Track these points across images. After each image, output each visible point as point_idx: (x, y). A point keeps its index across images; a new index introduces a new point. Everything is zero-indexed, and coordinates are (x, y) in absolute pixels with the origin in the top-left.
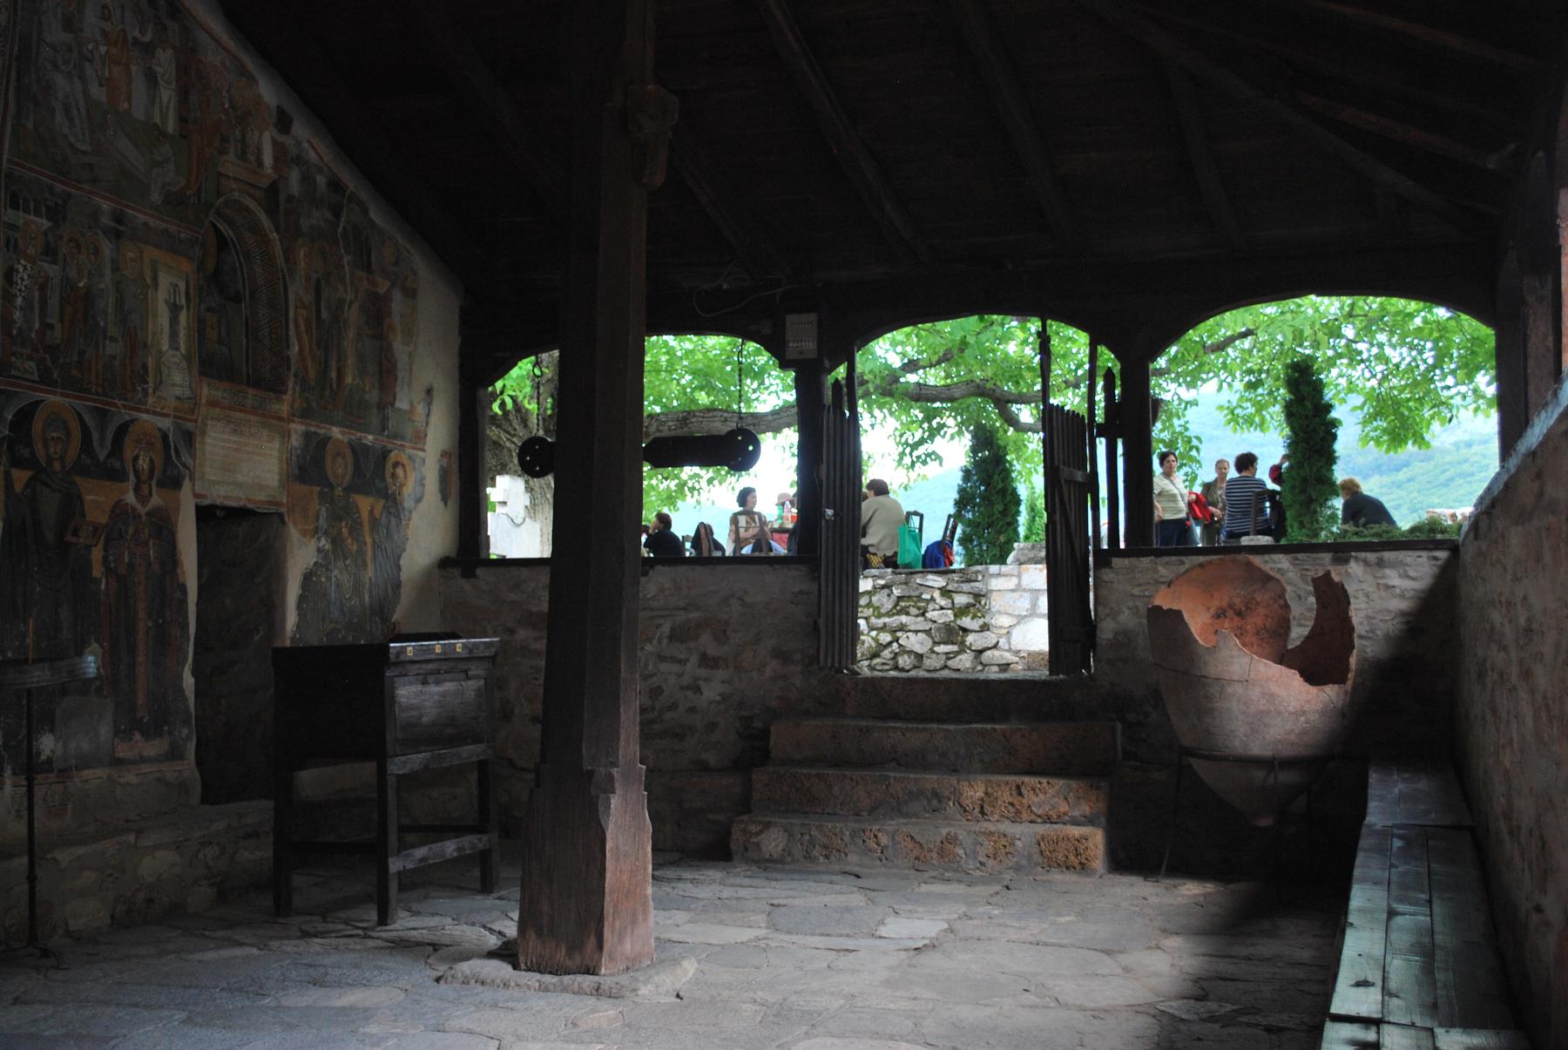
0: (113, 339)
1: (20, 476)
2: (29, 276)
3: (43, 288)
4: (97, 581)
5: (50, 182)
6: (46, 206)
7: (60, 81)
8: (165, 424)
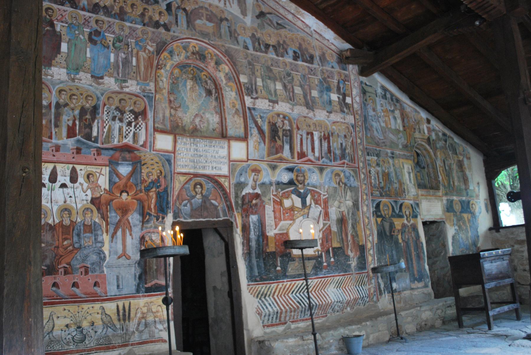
0: (396, 183)
1: (379, 220)
3: (378, 174)
4: (401, 244)
7: (374, 124)
8: (411, 202)
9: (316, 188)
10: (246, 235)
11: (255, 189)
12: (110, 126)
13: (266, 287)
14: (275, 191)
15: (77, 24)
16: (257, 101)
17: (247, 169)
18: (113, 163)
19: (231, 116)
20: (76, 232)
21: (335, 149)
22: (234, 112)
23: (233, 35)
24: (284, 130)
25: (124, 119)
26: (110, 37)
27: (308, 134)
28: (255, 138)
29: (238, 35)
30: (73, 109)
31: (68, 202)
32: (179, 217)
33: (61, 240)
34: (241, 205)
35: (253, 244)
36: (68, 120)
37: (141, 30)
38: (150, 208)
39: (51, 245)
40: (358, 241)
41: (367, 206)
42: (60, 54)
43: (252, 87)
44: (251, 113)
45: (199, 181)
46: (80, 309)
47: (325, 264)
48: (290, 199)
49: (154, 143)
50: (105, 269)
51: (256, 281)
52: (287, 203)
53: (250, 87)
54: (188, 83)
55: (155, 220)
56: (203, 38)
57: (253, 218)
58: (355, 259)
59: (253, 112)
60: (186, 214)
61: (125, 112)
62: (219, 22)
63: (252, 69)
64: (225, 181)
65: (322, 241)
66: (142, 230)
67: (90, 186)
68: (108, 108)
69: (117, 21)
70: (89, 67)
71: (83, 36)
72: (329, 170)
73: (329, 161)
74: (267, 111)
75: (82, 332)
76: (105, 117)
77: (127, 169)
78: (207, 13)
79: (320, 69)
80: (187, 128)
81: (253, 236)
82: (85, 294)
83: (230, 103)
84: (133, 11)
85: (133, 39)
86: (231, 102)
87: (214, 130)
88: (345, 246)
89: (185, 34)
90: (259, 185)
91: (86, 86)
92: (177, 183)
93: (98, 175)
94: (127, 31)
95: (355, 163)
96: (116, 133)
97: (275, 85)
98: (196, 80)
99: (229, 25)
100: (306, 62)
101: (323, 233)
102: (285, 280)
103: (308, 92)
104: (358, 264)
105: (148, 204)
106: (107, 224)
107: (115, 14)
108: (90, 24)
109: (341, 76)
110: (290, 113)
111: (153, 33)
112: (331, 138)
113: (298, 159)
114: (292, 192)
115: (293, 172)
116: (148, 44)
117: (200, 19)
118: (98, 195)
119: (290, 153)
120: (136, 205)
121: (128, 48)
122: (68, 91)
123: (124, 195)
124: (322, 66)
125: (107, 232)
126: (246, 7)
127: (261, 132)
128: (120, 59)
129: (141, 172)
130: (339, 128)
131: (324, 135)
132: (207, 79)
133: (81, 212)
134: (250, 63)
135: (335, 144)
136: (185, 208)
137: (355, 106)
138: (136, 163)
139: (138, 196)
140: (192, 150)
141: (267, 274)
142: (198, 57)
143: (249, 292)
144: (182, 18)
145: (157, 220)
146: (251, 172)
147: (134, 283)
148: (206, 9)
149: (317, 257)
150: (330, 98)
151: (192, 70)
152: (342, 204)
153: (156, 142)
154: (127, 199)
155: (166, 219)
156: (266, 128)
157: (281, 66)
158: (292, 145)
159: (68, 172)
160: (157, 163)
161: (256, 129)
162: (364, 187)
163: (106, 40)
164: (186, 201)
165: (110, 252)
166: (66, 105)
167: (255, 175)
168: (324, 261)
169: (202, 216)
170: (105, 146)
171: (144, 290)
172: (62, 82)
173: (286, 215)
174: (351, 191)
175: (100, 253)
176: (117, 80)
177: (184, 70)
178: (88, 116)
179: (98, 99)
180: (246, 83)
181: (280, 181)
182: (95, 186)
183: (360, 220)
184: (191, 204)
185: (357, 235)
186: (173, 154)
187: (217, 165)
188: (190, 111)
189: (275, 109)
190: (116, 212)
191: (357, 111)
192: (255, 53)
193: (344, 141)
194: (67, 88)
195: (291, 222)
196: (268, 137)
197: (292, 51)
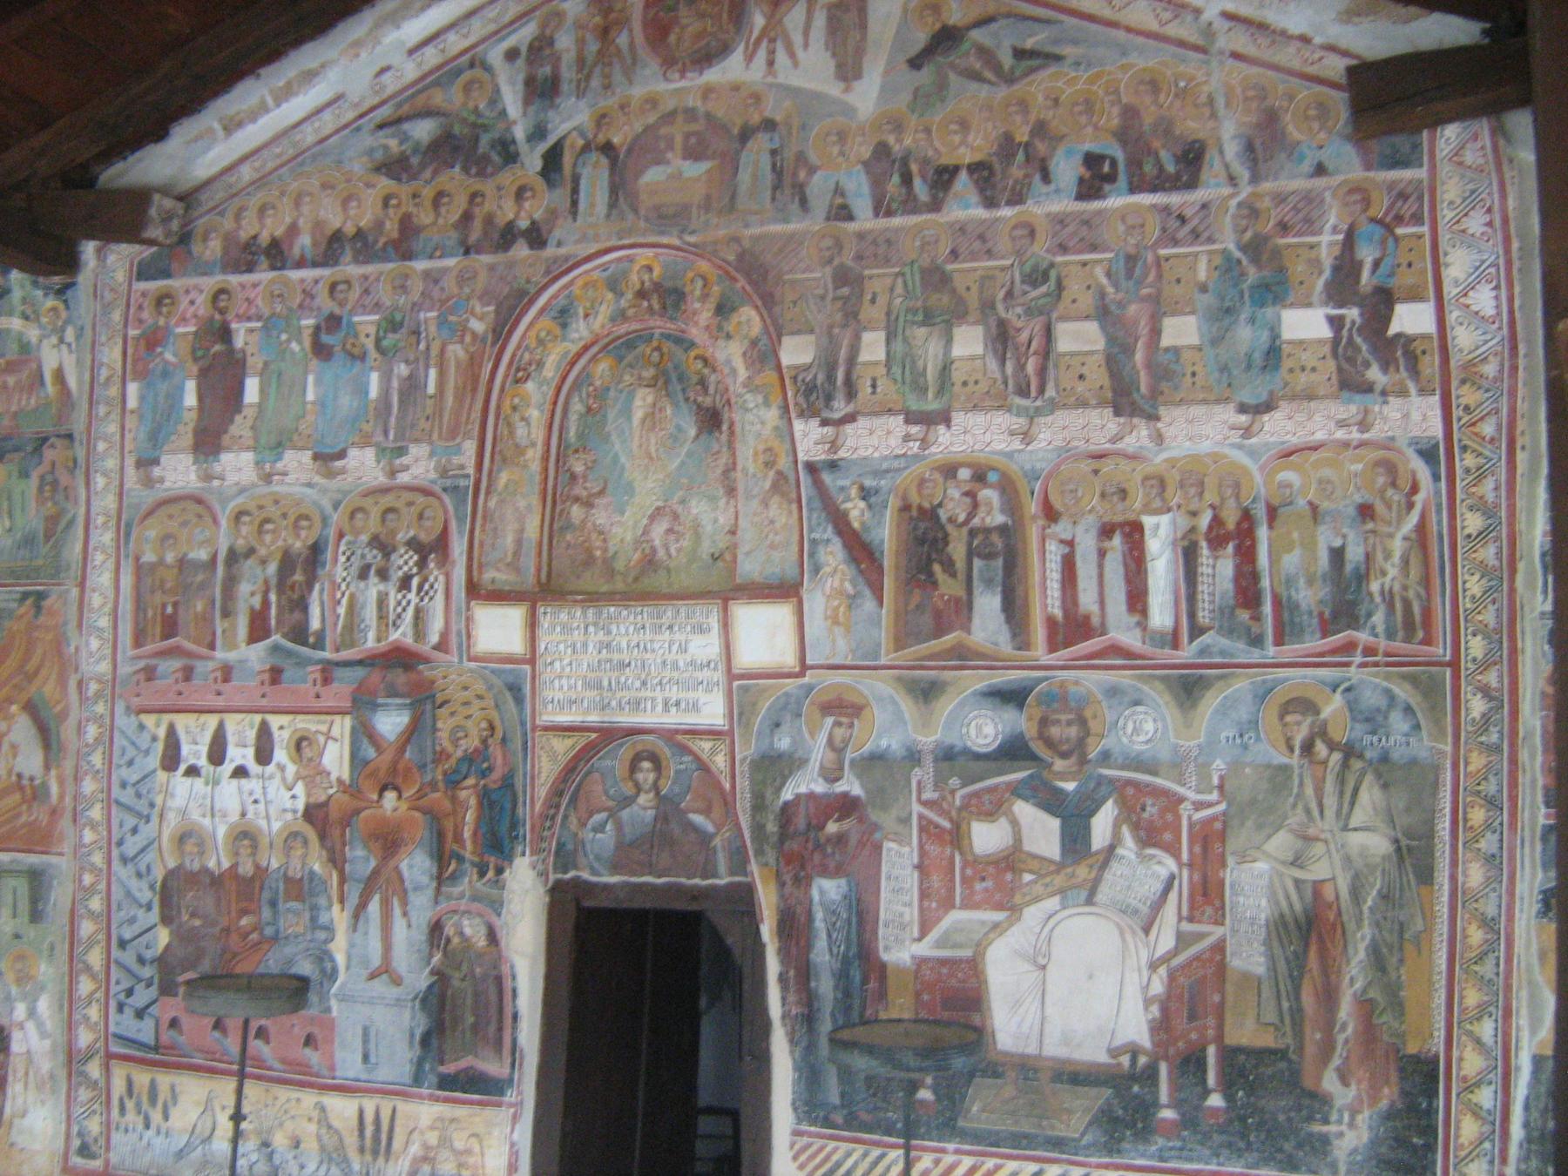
9: (1155, 773)
10: (794, 950)
11: (837, 779)
12: (352, 597)
13: (865, 1155)
14: (930, 786)
15: (285, 312)
16: (849, 429)
17: (799, 704)
18: (362, 704)
19: (755, 503)
20: (266, 895)
21: (1290, 582)
22: (768, 484)
23: (787, 179)
24: (973, 533)
25: (391, 572)
26: (367, 322)
27: (1107, 531)
28: (830, 584)
29: (812, 170)
30: (264, 562)
31: (250, 815)
32: (576, 867)
33: (234, 914)
34: (775, 839)
35: (825, 986)
36: (253, 594)
37: (454, 273)
38: (458, 838)
39: (214, 924)
40: (1402, 1036)
41: (1491, 860)
42: (240, 412)
43: (831, 378)
44: (818, 484)
45: (649, 747)
46: (270, 1102)
47: (1168, 1114)
49: (469, 636)
50: (334, 1003)
51: (827, 1122)
52: (987, 837)
53: (821, 378)
54: (638, 402)
55: (475, 877)
56: (662, 233)
57: (828, 890)
58: (1363, 1118)
59: (827, 477)
60: (598, 858)
61: (394, 549)
62: (737, 145)
63: (846, 299)
64: (713, 752)
65: (1165, 1010)
66: (436, 902)
67: (304, 773)
68: (349, 543)
69: (391, 266)
70: (309, 431)
71: (300, 342)
72: (1241, 685)
73: (1241, 645)
74: (896, 464)
75: (270, 1156)
76: (340, 573)
77: (398, 720)
78: (694, 127)
79: (1233, 203)
80: (620, 565)
81: (822, 954)
82: (284, 1061)
83: (756, 454)
84: (438, 215)
85: (431, 310)
86: (761, 447)
87: (715, 558)
88: (1310, 1050)
89: (596, 238)
91: (297, 489)
92: (544, 759)
93: (322, 739)
94: (417, 287)
95: (1427, 641)
96: (370, 613)
97: (949, 341)
98: (667, 382)
99: (776, 145)
100: (1154, 189)
101: (1172, 977)
102: (951, 1146)
103: (1143, 329)
104: (1375, 1142)
105: (456, 826)
106: (343, 880)
107: (386, 244)
108: (318, 301)
109: (1367, 202)
110: (1010, 455)
111: (492, 268)
112: (1262, 533)
113: (1053, 647)
114: (1016, 791)
116: (473, 313)
117: (658, 163)
118: (323, 798)
119: (1005, 628)
120: (421, 829)
121: (418, 343)
122: (255, 512)
123: (390, 796)
124: (1255, 178)
125: (342, 901)
126: (864, 38)
127: (861, 551)
128: (395, 384)
129: (435, 730)
130: (1327, 472)
131: (1217, 521)
132: (706, 371)
133: (279, 842)
134: (843, 277)
136: (599, 836)
137: (1464, 338)
138: (419, 701)
139: (424, 802)
140: (590, 648)
141: (876, 1108)
142: (656, 307)
143: (795, 1158)
144: (595, 180)
145: (482, 874)
146: (817, 715)
147: (409, 1055)
148: (691, 114)
149: (1122, 1077)
150: (1275, 336)
151: (658, 349)
152: (1319, 848)
153: (474, 633)
154: (395, 810)
155: (507, 874)
156: (886, 534)
157: (1003, 244)
158: (1020, 591)
159: (251, 735)
160: (480, 697)
161: (837, 546)
162: (1477, 761)
163: (356, 336)
164: (604, 815)
165: (349, 958)
166: (251, 551)
167: (838, 724)
168: (1164, 1097)
169: (650, 869)
170: (346, 654)
171: (433, 1079)
172: (242, 491)
173: (979, 886)
174: (1385, 786)
175: (322, 954)
176: (381, 451)
177: (630, 358)
178: (298, 577)
179: (325, 520)
180: (807, 368)
181: (959, 744)
182: (313, 772)
183: (1429, 929)
184: (619, 827)
185: (1398, 1006)
186: (527, 668)
187: (682, 695)
188: (637, 499)
189: (933, 449)
190: (366, 846)
191: (1469, 365)
192: (882, 223)
193: (1351, 536)
194: (252, 506)
195: (999, 916)
196: (897, 568)
197: (1079, 159)
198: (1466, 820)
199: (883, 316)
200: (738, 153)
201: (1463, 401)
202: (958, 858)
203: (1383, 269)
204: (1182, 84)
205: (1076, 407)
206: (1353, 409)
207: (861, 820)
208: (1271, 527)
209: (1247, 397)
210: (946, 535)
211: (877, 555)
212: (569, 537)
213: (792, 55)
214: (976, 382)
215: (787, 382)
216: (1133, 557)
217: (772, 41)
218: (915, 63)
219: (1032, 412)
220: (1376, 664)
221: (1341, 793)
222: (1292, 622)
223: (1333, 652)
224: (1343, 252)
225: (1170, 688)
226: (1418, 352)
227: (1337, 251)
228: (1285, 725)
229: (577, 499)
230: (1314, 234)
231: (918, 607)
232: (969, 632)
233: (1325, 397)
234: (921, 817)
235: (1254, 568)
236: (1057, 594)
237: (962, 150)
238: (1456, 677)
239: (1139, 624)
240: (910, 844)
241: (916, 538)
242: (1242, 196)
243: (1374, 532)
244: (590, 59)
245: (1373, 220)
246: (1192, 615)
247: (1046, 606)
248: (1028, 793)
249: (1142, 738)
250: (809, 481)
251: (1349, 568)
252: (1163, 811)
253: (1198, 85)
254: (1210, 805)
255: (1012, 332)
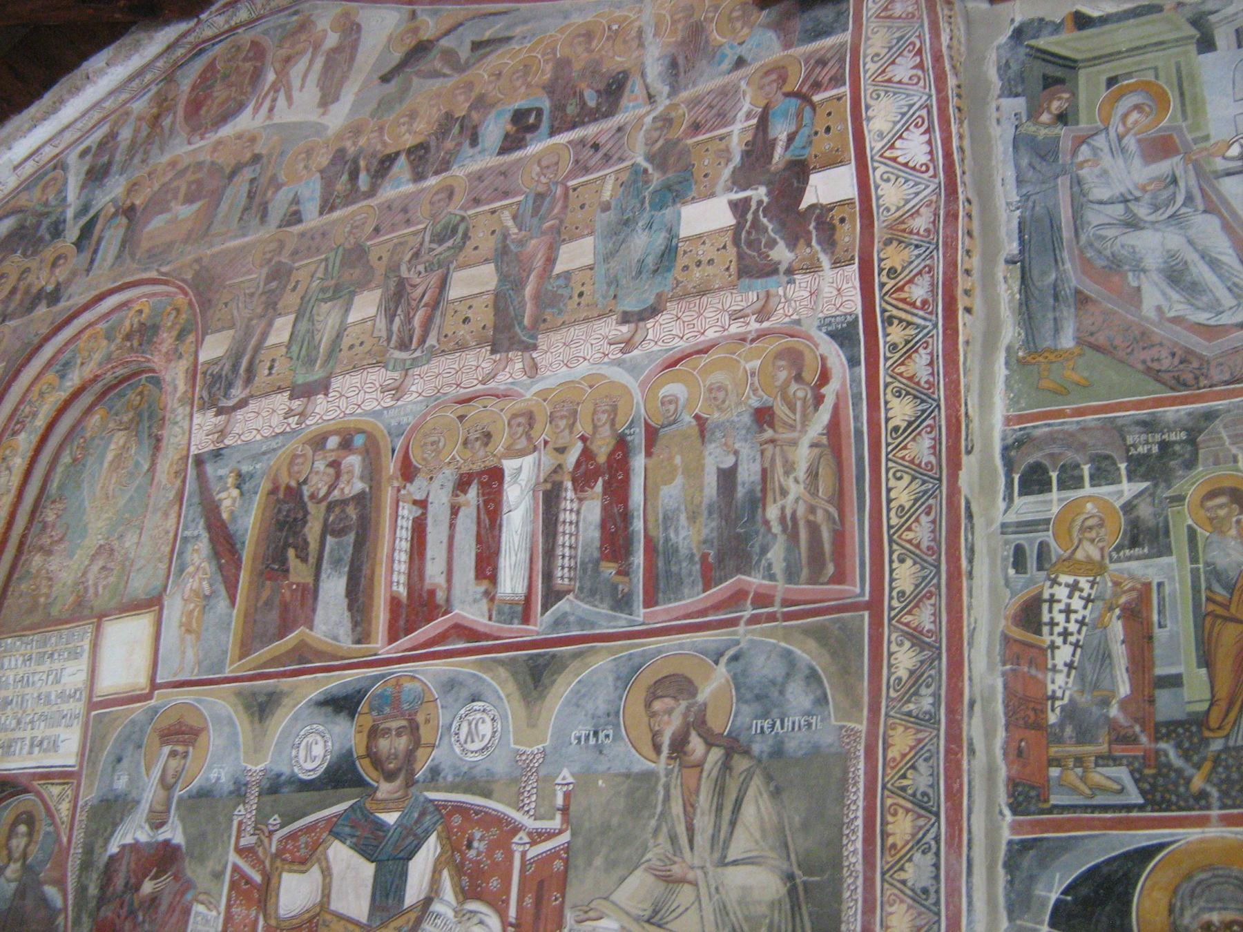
2: (1088, 600)
5: (1142, 413)
6: (1129, 459)
9: (488, 794)
11: (162, 824)
16: (239, 415)
17: (142, 730)
21: (668, 520)
27: (462, 484)
28: (191, 584)
34: (92, 904)
43: (235, 367)
44: (201, 477)
48: (315, 872)
53: (227, 367)
64: (61, 798)
72: (602, 663)
73: (604, 610)
74: (274, 445)
79: (648, 119)
90: (181, 799)
103: (539, 263)
109: (783, 79)
110: (377, 414)
112: (639, 462)
113: (393, 637)
114: (334, 829)
115: (352, 714)
119: (347, 614)
124: (674, 90)
130: (719, 377)
131: (587, 454)
135: (671, 493)
152: (685, 895)
158: (366, 570)
162: (902, 741)
167: (173, 754)
174: (776, 794)
181: (286, 770)
193: (745, 450)
196: (254, 559)
198: (885, 835)
199: (299, 301)
200: (225, 187)
201: (887, 265)
202: (261, 922)
203: (799, 141)
204: (615, 27)
205: (454, 351)
206: (752, 296)
207: (176, 877)
208: (649, 454)
209: (631, 304)
210: (306, 513)
211: (238, 546)
212: (23, 587)
213: (289, 98)
214: (362, 344)
215: (199, 377)
216: (488, 512)
217: (277, 91)
218: (385, 79)
219: (408, 363)
220: (772, 617)
221: (719, 809)
222: (668, 573)
223: (717, 607)
224: (755, 136)
225: (514, 674)
226: (836, 222)
227: (749, 136)
228: (653, 715)
229: (41, 548)
230: (725, 126)
231: (266, 604)
232: (311, 628)
233: (720, 289)
234: (236, 868)
235: (626, 506)
236: (404, 567)
237: (407, 136)
238: (877, 623)
239: (486, 593)
240: (217, 907)
241: (278, 521)
242: (660, 109)
243: (772, 441)
244: (139, 141)
245: (787, 95)
246: (548, 576)
247: (392, 583)
248: (347, 830)
249: (477, 745)
250: (195, 473)
251: (741, 492)
252: (490, 851)
253: (632, 22)
254: (550, 835)
255: (409, 288)
